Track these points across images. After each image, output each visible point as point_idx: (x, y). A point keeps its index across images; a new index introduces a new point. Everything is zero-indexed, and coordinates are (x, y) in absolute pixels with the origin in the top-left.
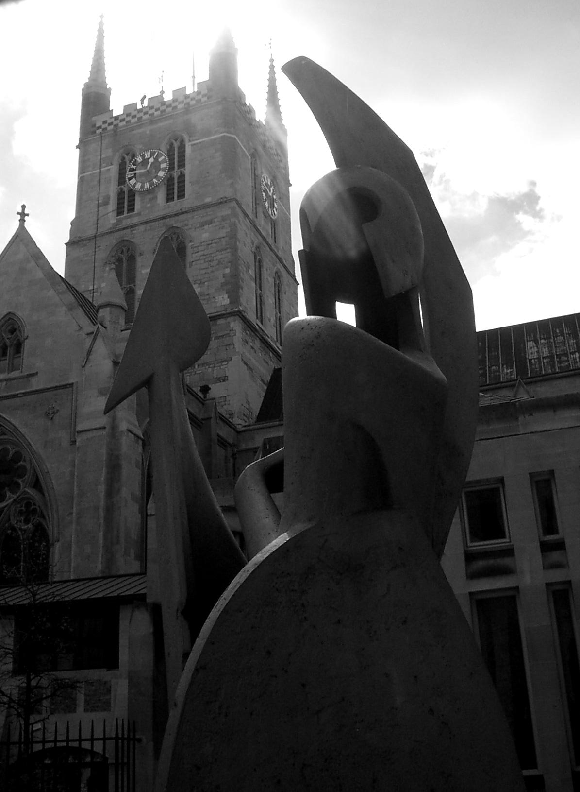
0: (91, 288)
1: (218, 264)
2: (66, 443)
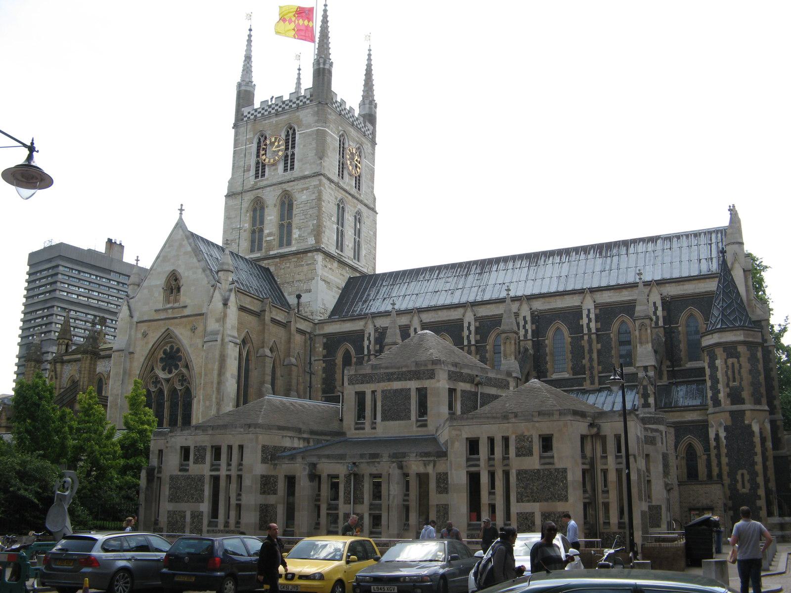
0: (239, 227)
2: (200, 346)
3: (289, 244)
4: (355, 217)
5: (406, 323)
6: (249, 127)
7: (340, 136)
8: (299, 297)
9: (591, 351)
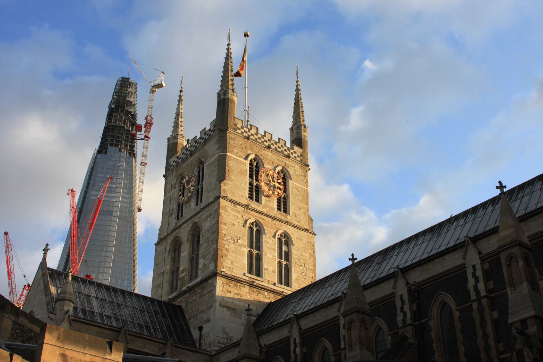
0: (163, 271)
1: (211, 243)
3: (196, 277)
4: (280, 240)
5: (287, 336)
6: (174, 174)
8: (201, 329)
9: (483, 324)
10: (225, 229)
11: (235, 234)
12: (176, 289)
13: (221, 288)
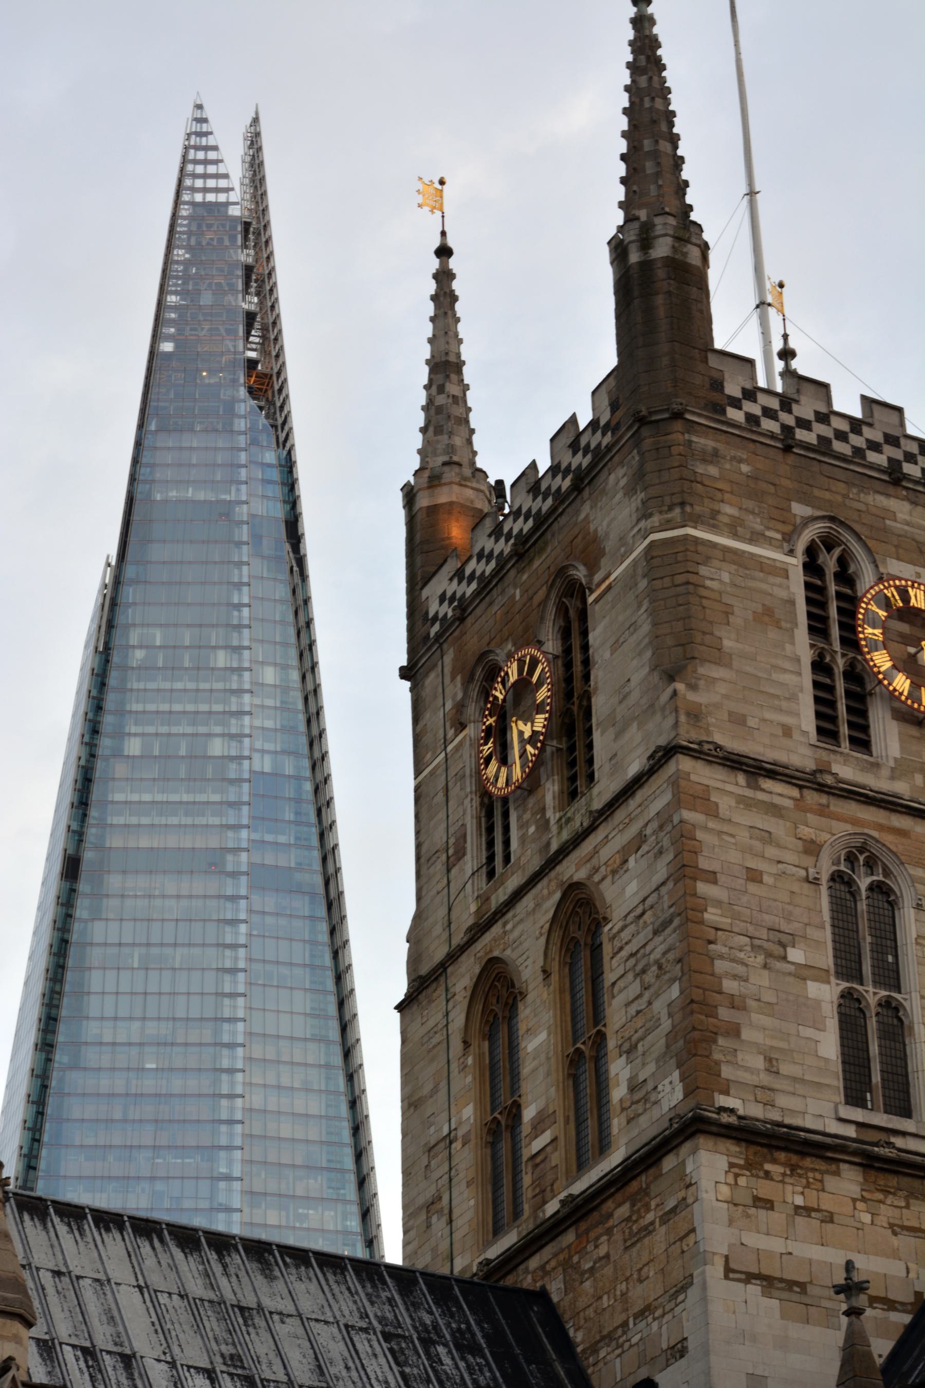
0: (445, 1131)
1: (658, 977)
7: (811, 551)
10: (718, 903)
11: (768, 919)
12: (517, 1214)
13: (725, 1191)
